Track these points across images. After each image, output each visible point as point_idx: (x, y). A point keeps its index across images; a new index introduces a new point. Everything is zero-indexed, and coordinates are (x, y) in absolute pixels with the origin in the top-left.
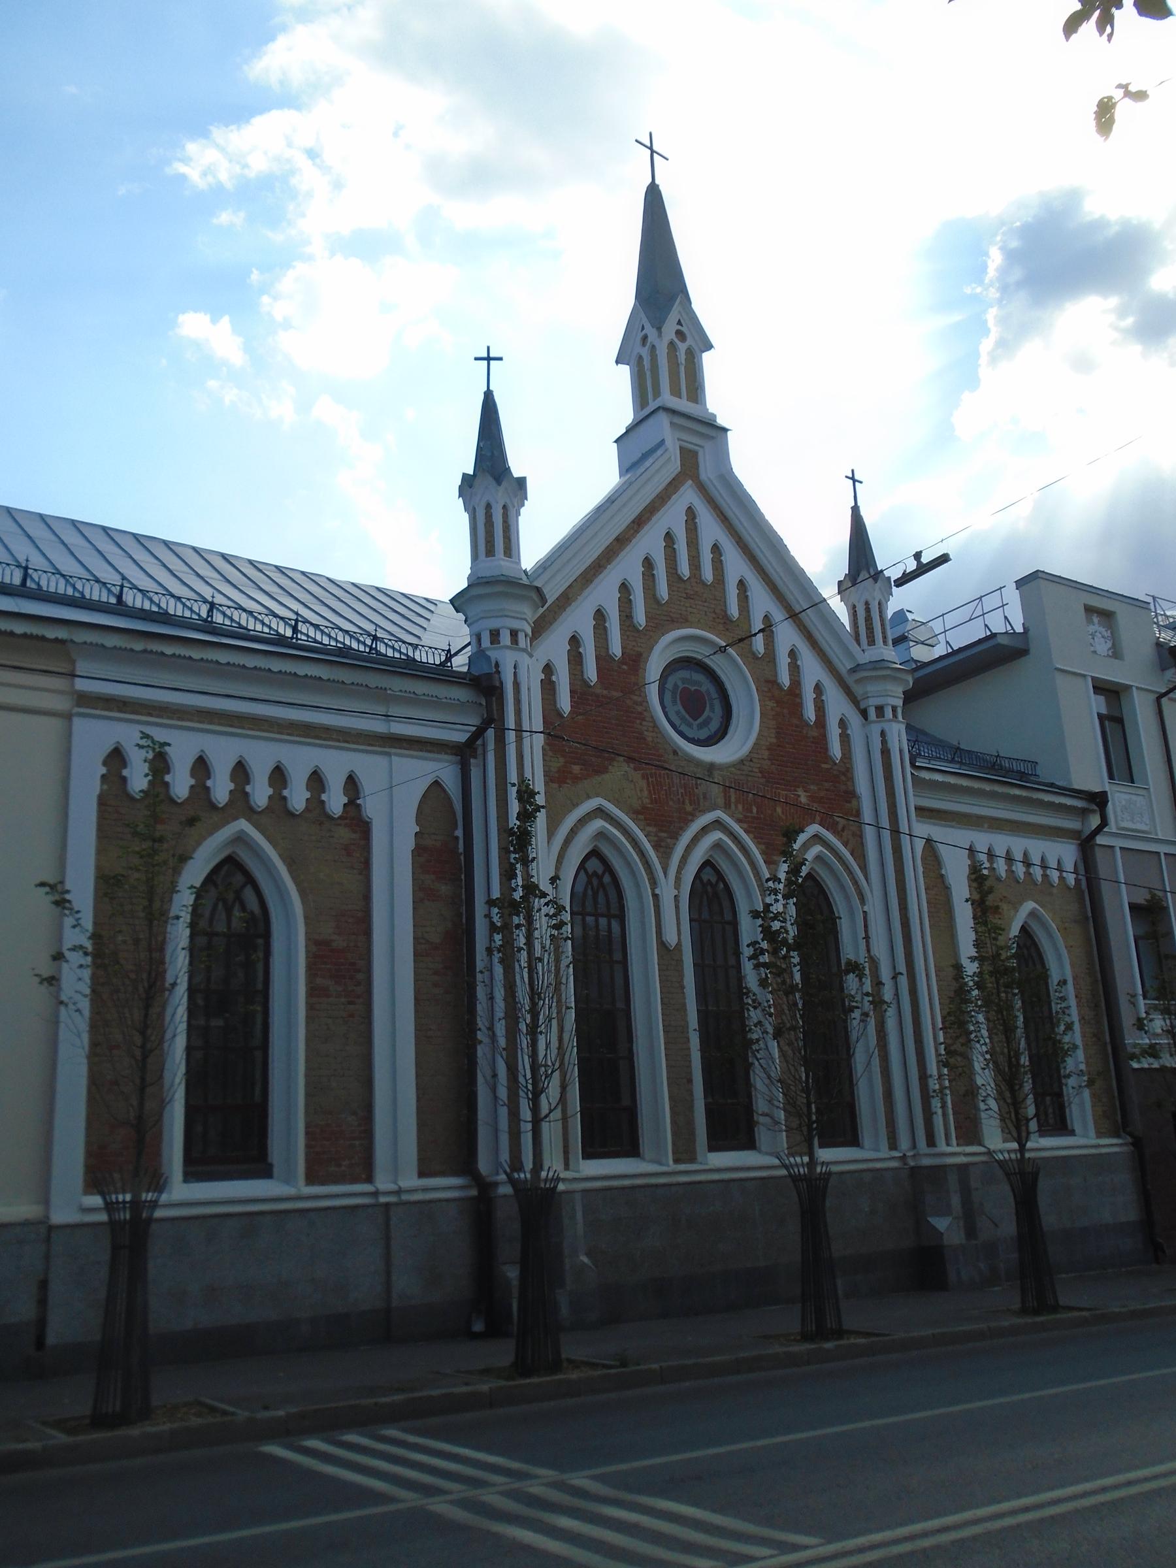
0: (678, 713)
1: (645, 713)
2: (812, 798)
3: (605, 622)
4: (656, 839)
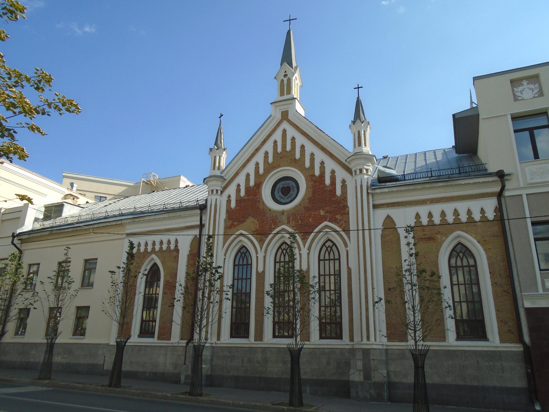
0: (280, 196)
2: (327, 212)
4: (260, 239)
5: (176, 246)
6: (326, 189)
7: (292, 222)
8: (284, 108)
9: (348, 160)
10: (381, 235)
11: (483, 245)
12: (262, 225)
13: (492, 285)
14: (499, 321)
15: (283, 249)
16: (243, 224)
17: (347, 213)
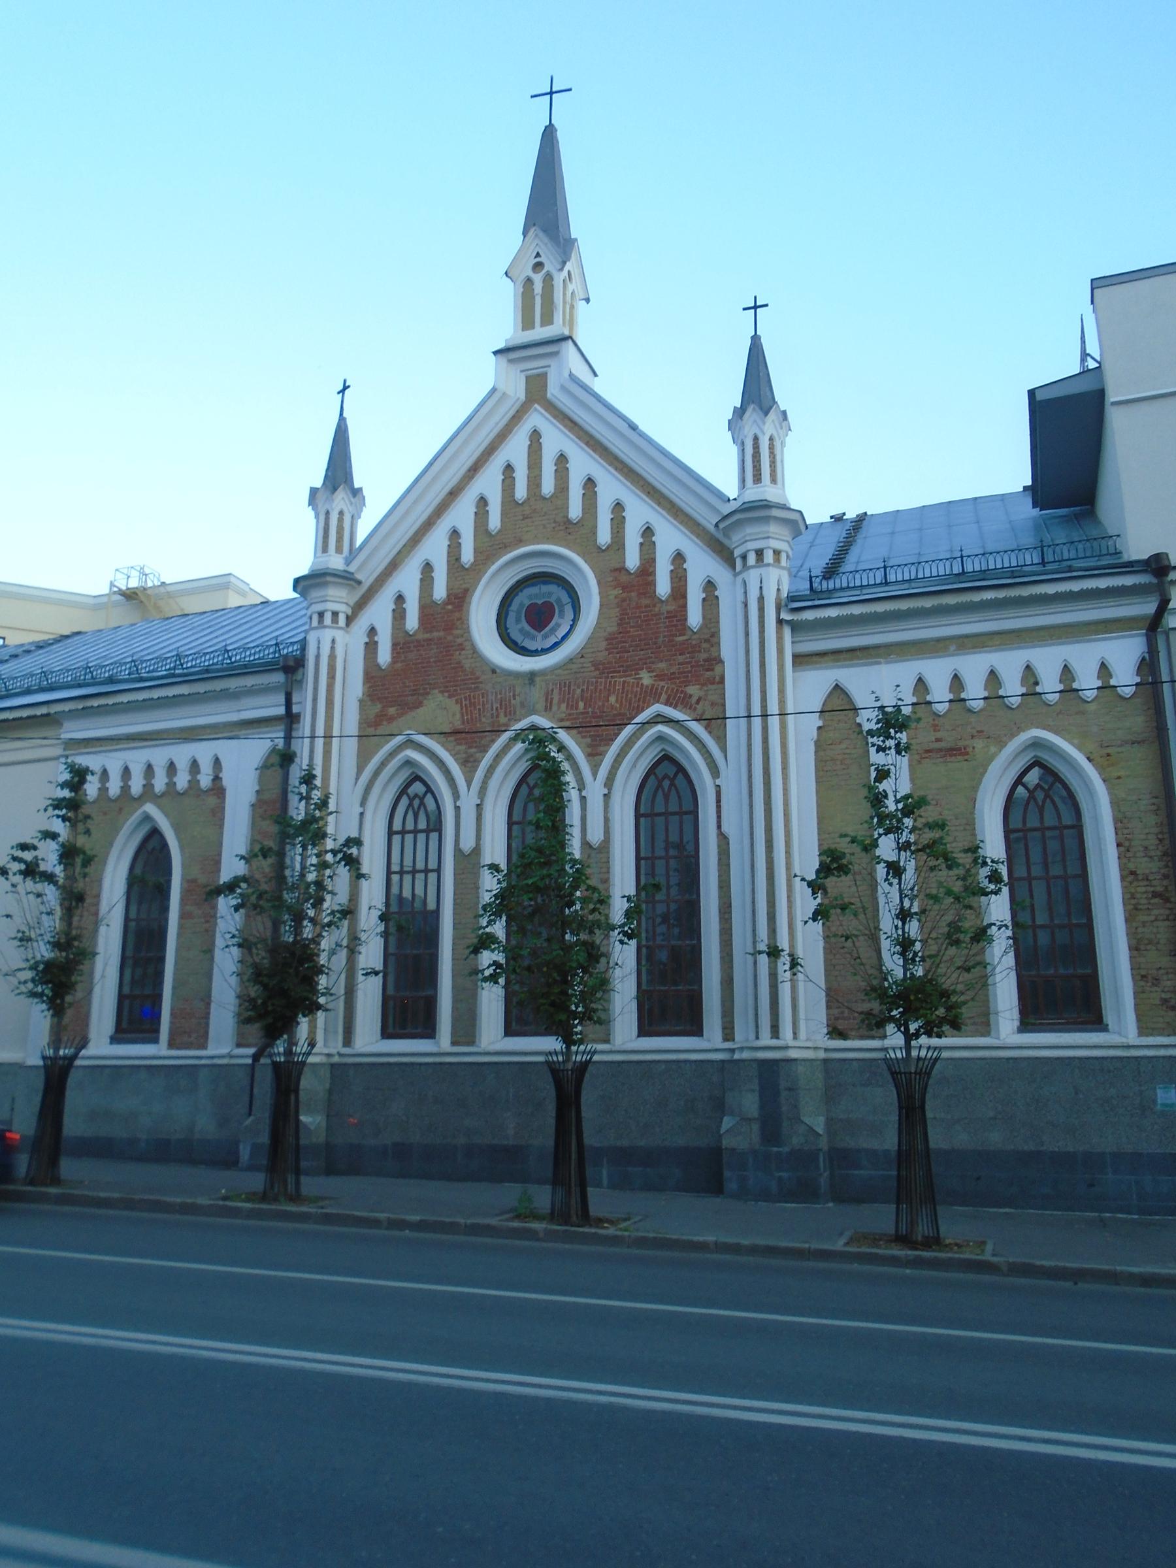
0: (521, 630)
1: (467, 643)
2: (660, 677)
5: (217, 778)
6: (657, 609)
7: (559, 708)
9: (721, 526)
10: (816, 743)
11: (1100, 769)
13: (1123, 878)
14: (1138, 978)
15: (532, 785)
16: (413, 714)
17: (717, 679)
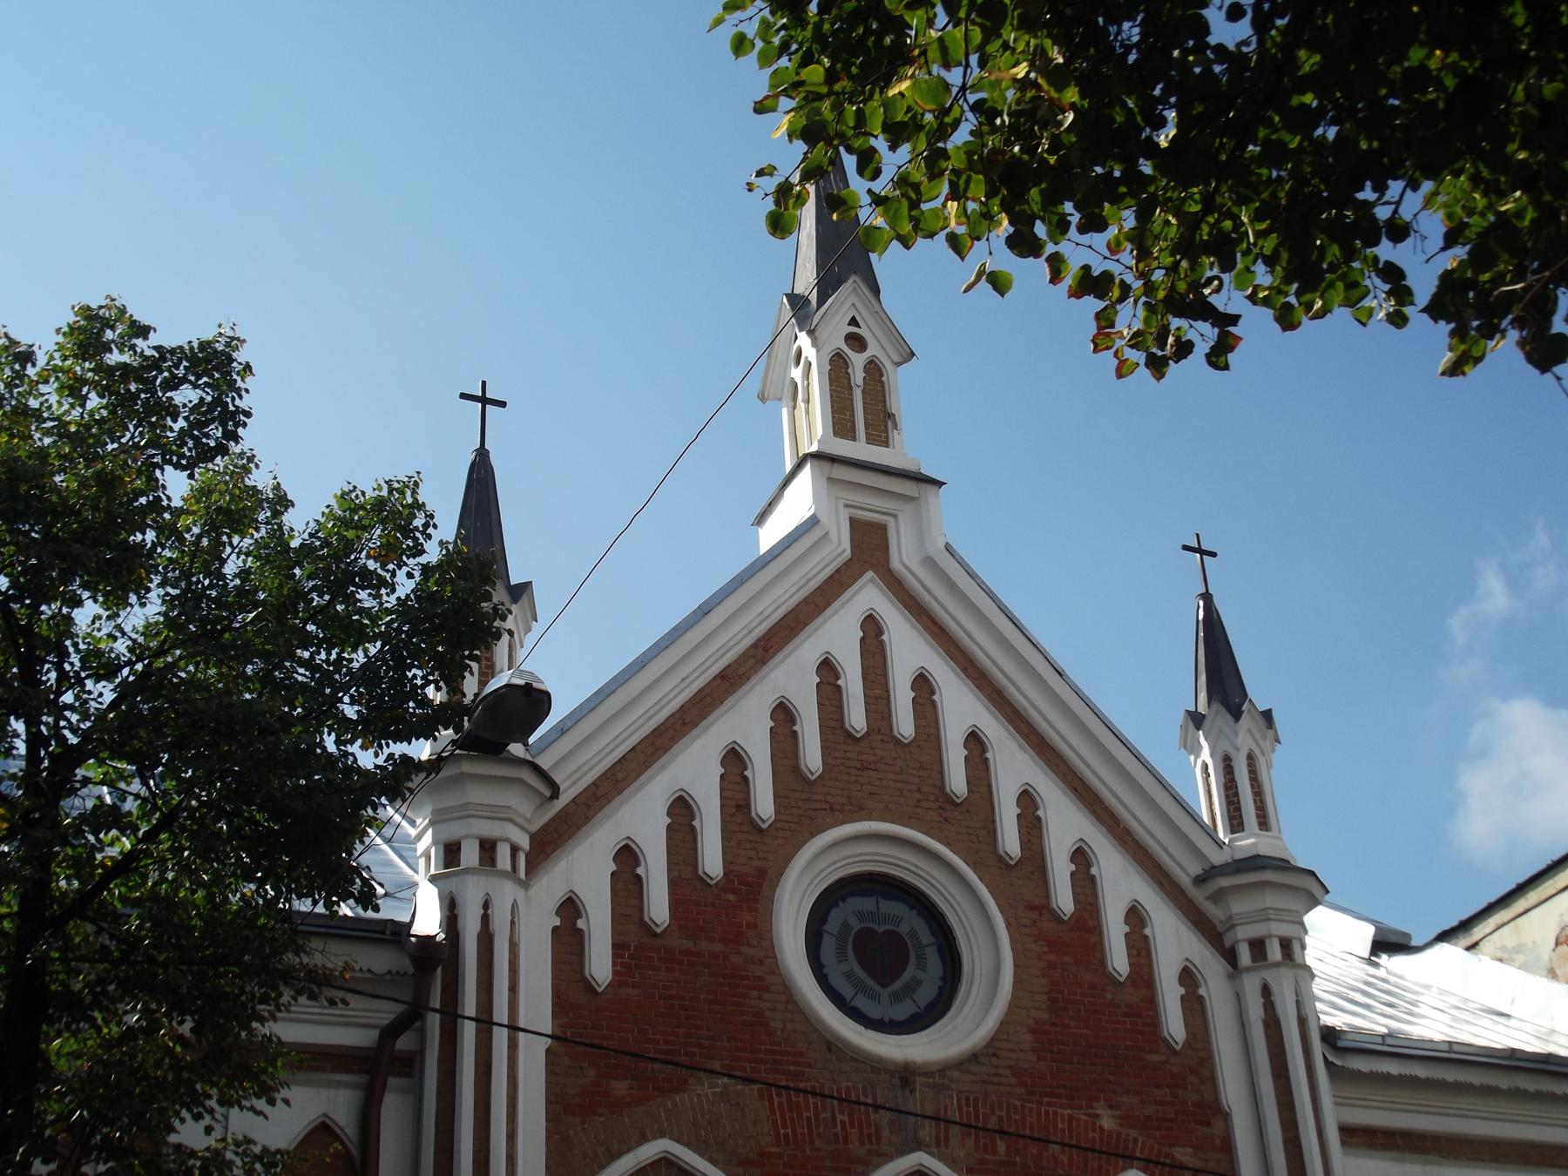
0: (849, 975)
3: (693, 817)
8: (872, 507)
12: (794, 1131)
17: (1218, 1142)
